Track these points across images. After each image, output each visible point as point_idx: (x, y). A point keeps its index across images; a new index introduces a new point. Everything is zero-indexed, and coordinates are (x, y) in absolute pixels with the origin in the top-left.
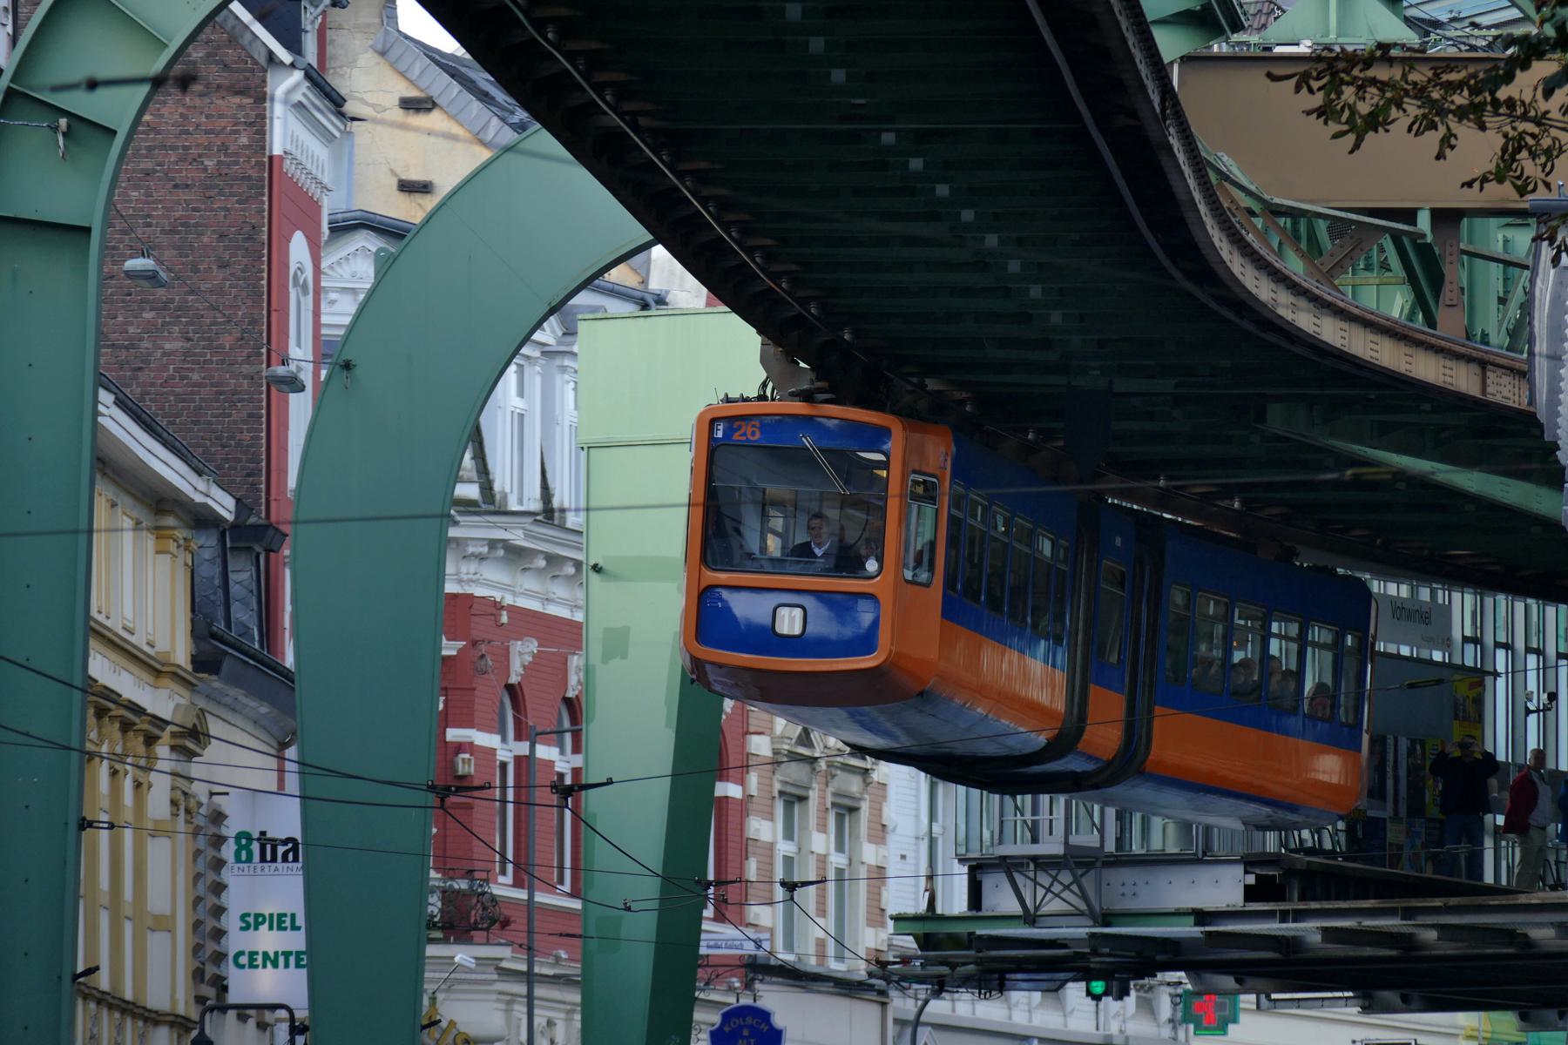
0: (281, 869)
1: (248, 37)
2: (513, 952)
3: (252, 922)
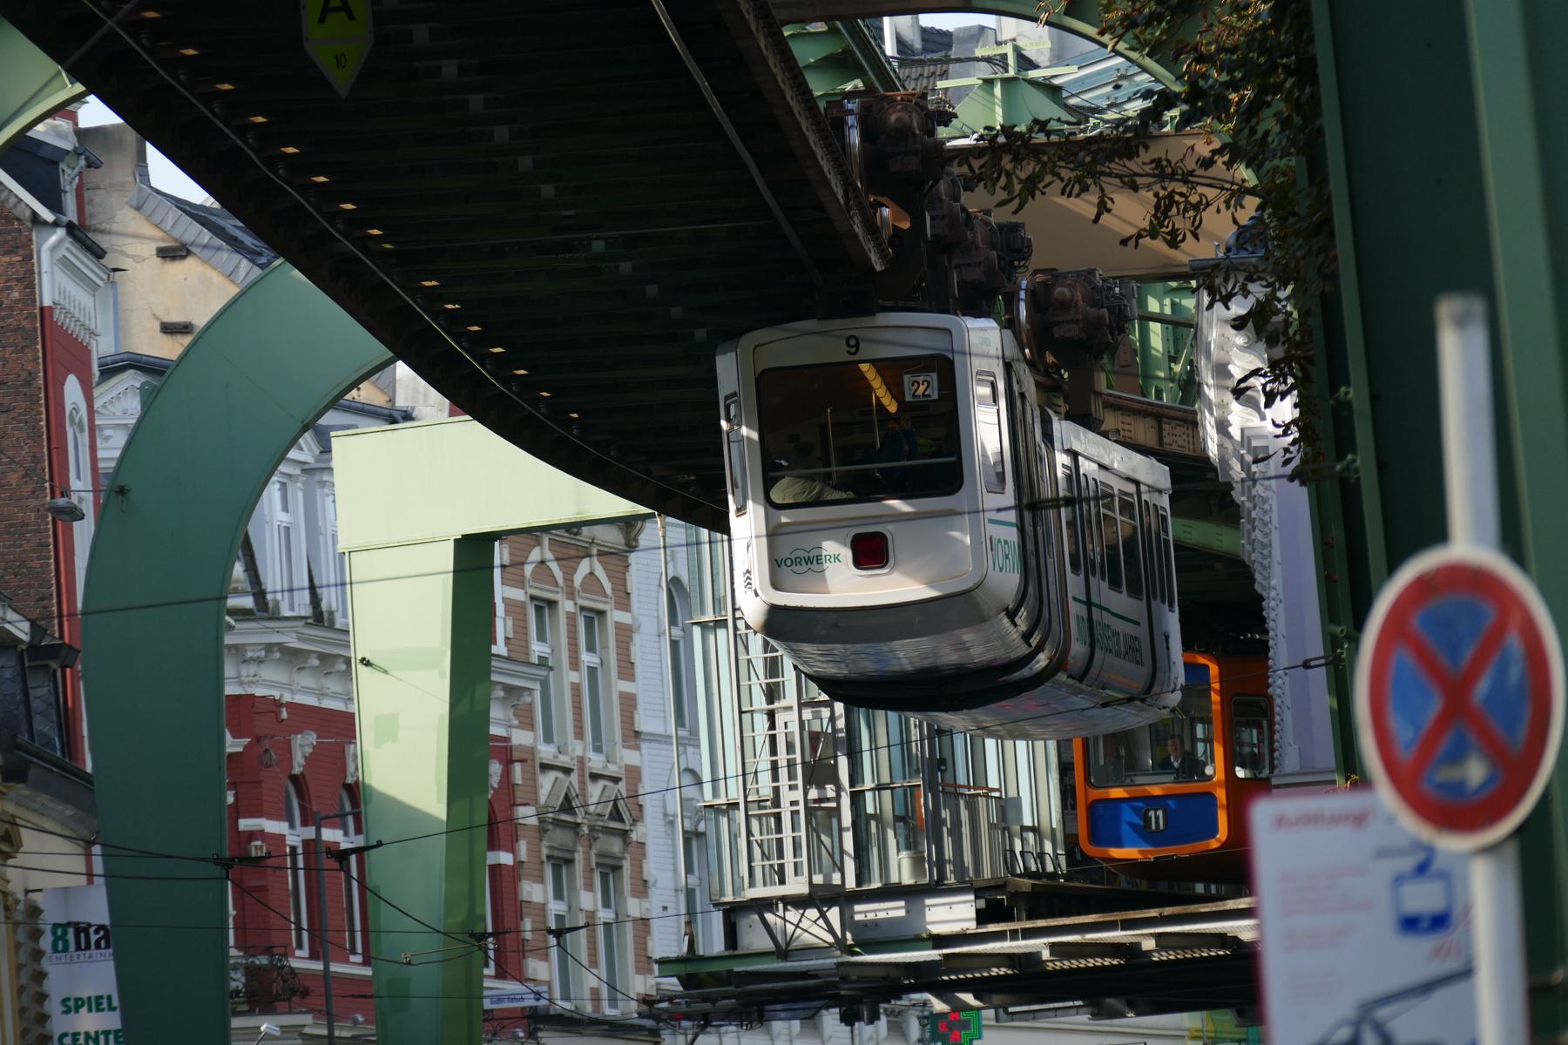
0: (94, 955)
1: (12, 200)
2: (314, 1018)
3: (73, 1005)
